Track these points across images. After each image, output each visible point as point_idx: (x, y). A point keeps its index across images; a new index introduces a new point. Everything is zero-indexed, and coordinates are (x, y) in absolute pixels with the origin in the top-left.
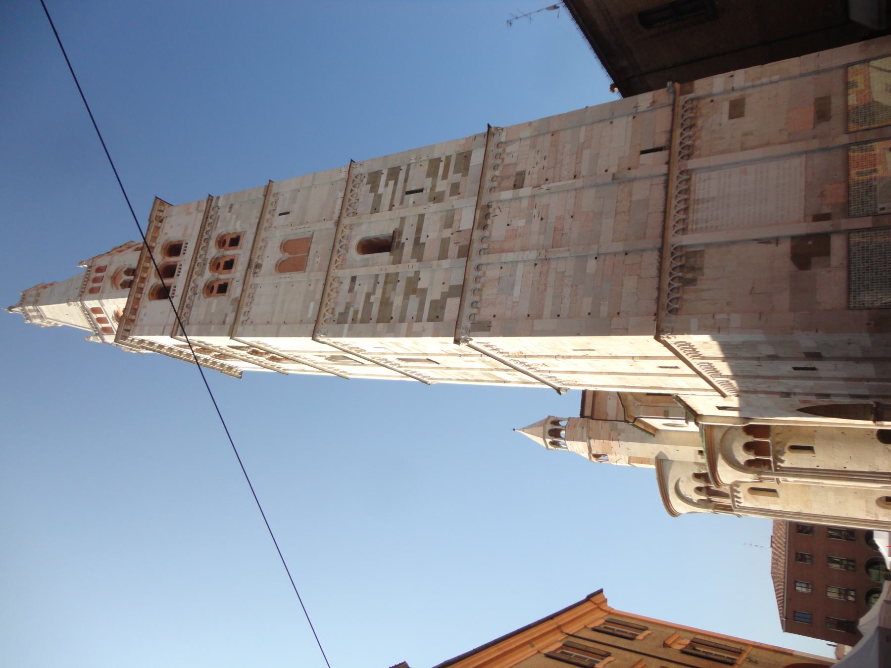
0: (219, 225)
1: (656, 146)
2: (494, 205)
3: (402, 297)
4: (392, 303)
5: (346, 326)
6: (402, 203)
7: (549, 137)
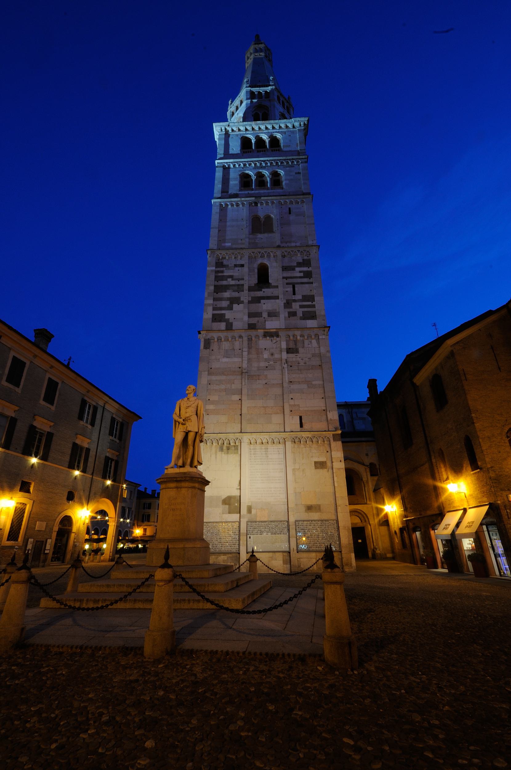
0: (287, 168)
1: (303, 424)
2: (278, 339)
3: (229, 296)
4: (226, 292)
5: (214, 268)
6: (287, 284)
7: (319, 363)
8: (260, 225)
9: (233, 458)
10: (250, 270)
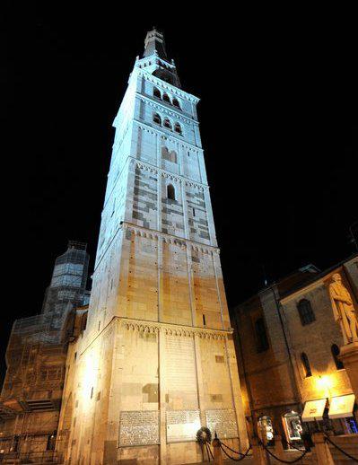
8: (166, 154)
9: (152, 346)
10: (163, 186)
